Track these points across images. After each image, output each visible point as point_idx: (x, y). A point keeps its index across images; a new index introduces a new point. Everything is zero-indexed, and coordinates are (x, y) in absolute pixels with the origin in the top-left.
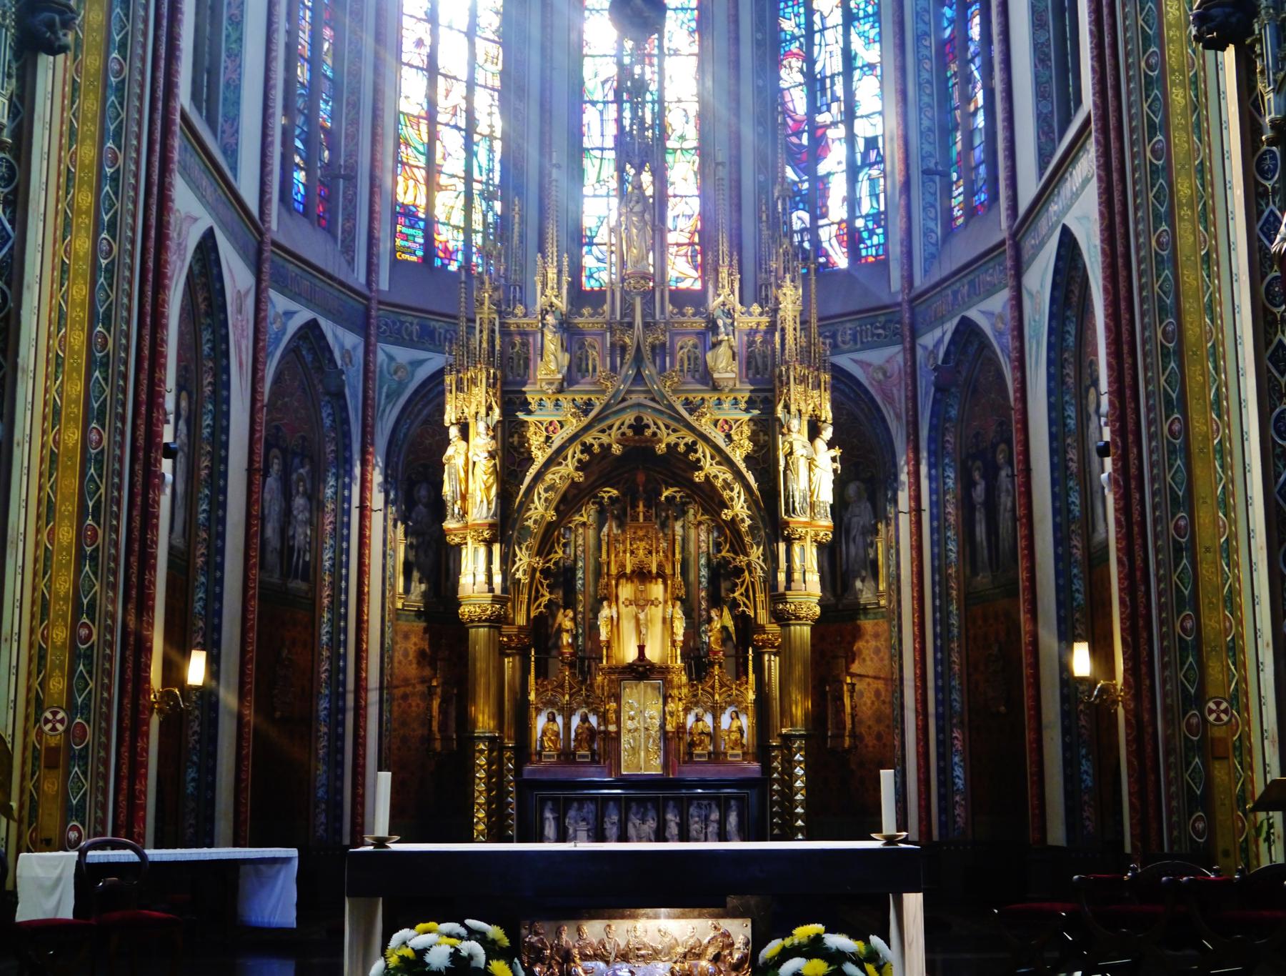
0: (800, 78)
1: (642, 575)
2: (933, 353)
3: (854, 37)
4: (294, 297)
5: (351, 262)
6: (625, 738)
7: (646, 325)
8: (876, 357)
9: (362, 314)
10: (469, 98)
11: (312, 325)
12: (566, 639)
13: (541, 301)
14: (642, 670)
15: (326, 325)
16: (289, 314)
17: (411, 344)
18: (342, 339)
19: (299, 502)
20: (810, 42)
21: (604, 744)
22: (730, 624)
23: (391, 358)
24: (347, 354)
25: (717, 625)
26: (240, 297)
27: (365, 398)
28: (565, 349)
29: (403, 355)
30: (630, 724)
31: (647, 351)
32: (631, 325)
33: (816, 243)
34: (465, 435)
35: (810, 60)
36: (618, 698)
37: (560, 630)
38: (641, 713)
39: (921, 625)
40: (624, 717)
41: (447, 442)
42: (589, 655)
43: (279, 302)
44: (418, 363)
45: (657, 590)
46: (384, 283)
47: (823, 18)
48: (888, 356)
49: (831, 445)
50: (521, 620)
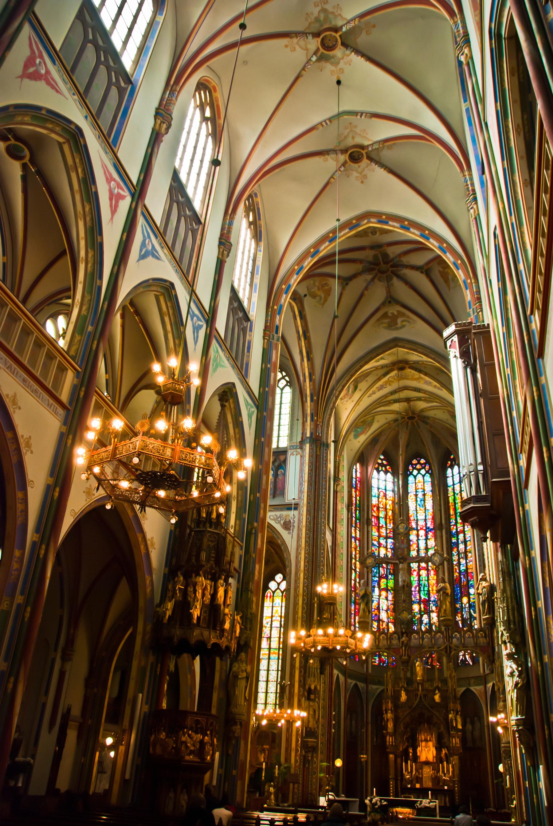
0: (460, 619)
1: (426, 740)
2: (489, 689)
3: (471, 611)
4: (351, 679)
5: (363, 667)
6: (424, 778)
7: (422, 690)
8: (479, 688)
9: (365, 679)
10: (387, 625)
11: (356, 685)
12: (411, 754)
13: (401, 685)
14: (427, 763)
15: (358, 683)
16: (351, 683)
17: (375, 684)
18: (361, 685)
19: (354, 722)
20: (462, 611)
21: (419, 779)
22: (447, 752)
23: (372, 688)
24: (363, 688)
25: (444, 752)
26: (342, 683)
27: (367, 697)
28: (406, 695)
29: (374, 687)
30: (424, 775)
31: (422, 696)
32: (419, 690)
33: (465, 658)
34: (386, 713)
35: (462, 616)
36: (422, 769)
37: (410, 752)
38: (427, 771)
39: (490, 753)
40: (423, 773)
41: (382, 714)
42: (416, 758)
43: (349, 681)
44: (378, 688)
45: (431, 744)
46: (370, 671)
47: (465, 605)
48: (481, 688)
49: (461, 715)
50: (401, 749)
